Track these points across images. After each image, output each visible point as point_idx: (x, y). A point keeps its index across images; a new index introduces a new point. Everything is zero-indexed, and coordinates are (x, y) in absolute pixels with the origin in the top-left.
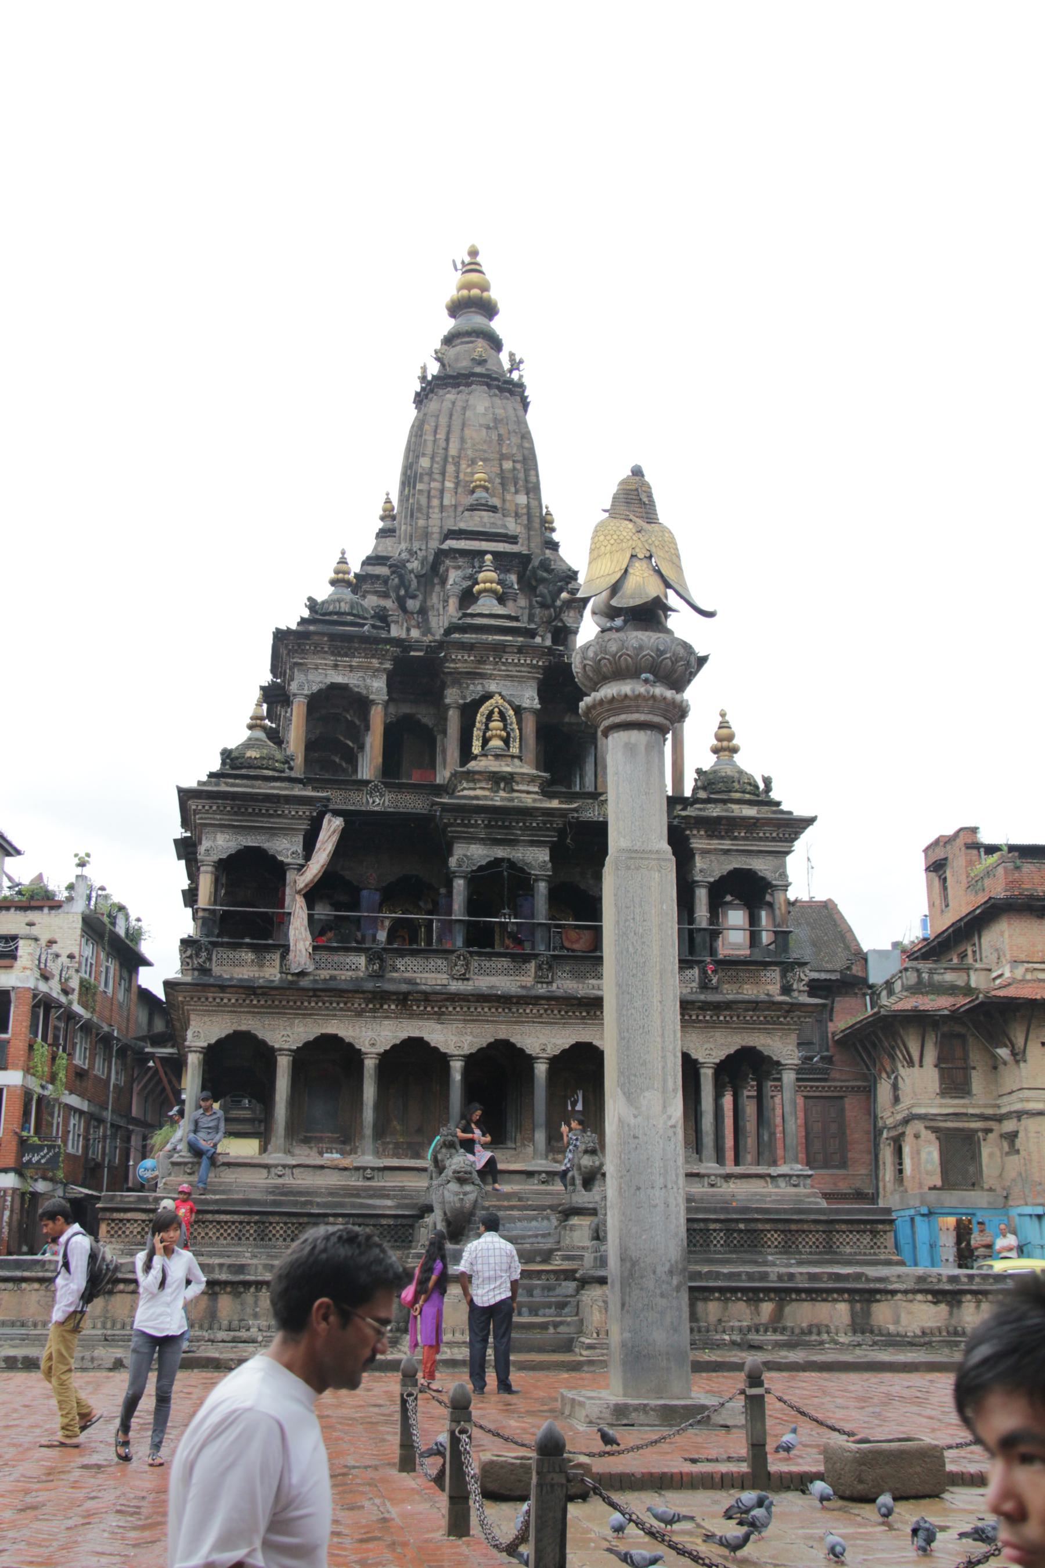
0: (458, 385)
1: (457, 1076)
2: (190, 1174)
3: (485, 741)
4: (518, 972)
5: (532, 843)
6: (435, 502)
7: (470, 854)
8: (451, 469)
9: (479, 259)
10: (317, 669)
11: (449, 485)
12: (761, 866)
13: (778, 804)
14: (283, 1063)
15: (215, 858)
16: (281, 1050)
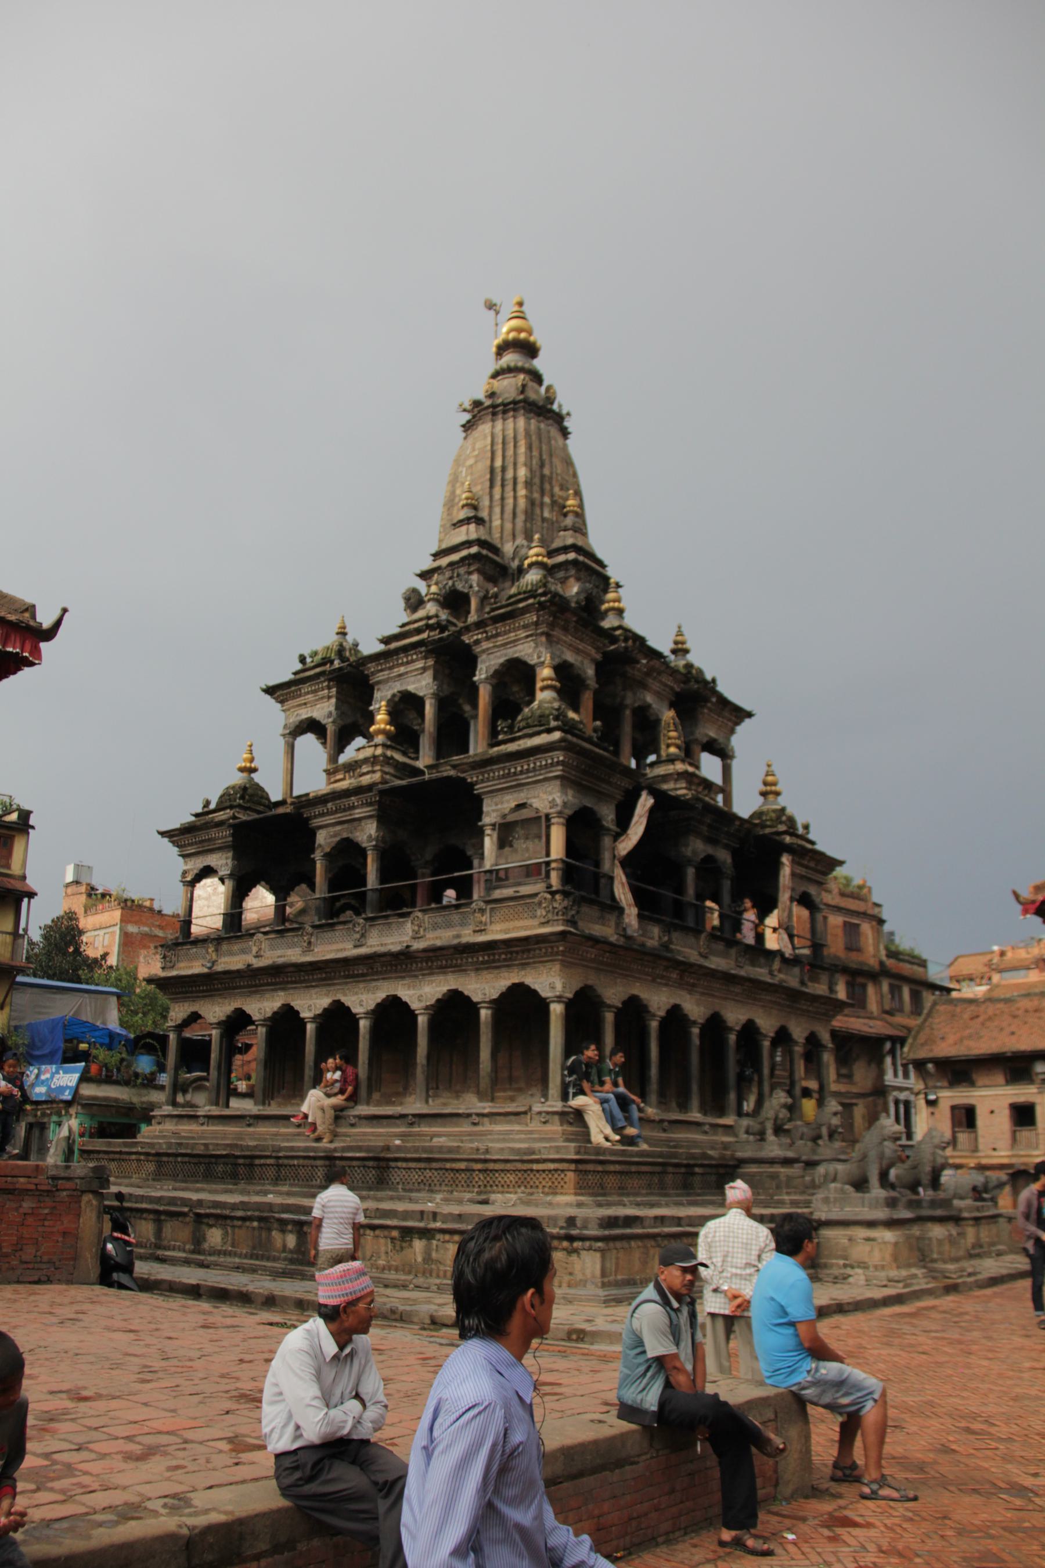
0: (539, 415)
1: (696, 1041)
2: (571, 1124)
3: (668, 746)
4: (725, 955)
5: (726, 847)
6: (538, 511)
7: (696, 847)
8: (547, 486)
9: (524, 309)
10: (557, 643)
11: (547, 500)
12: (812, 890)
13: (813, 843)
14: (609, 1017)
15: (569, 812)
16: (610, 1006)
